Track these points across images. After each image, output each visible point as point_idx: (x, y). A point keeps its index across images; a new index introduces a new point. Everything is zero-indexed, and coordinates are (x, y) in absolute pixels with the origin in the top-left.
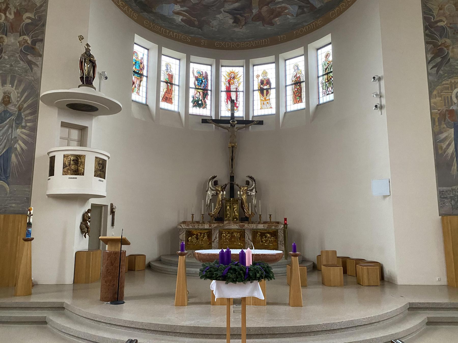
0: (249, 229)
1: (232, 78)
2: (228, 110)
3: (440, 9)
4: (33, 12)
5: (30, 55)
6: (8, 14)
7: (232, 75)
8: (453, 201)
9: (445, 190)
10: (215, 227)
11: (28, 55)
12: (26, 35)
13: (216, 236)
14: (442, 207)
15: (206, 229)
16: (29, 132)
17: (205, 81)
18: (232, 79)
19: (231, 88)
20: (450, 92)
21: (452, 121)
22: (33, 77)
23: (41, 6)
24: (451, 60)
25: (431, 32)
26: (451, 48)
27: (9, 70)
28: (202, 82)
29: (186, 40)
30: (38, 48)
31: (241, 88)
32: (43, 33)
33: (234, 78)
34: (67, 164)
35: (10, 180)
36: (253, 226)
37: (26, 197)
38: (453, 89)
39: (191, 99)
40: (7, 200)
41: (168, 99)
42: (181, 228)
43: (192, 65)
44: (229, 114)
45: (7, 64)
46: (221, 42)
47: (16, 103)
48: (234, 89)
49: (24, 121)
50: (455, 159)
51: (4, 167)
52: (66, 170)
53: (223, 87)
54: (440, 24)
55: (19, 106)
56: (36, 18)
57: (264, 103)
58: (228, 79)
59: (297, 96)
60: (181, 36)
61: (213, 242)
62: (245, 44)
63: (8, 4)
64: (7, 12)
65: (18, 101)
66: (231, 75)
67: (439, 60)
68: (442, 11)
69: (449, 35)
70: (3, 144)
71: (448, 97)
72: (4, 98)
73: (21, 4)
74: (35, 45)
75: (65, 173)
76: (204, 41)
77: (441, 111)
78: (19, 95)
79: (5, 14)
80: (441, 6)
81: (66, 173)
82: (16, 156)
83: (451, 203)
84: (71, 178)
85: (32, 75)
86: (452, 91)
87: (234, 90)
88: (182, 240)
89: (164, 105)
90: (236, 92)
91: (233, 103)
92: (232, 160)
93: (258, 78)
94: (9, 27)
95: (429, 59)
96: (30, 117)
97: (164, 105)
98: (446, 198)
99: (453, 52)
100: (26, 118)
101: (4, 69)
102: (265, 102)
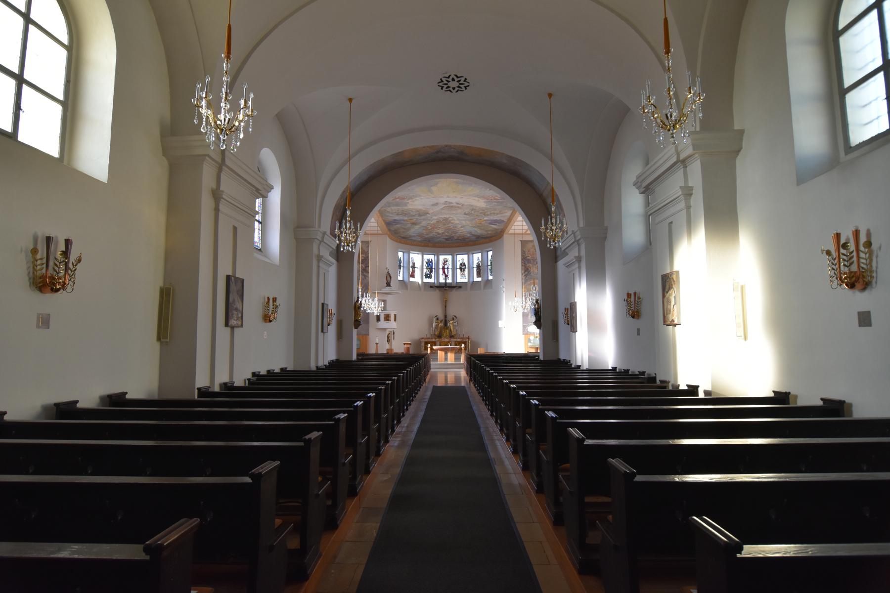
1: (445, 262)
3: (529, 251)
31: (450, 267)
33: (446, 261)
36: (455, 340)
39: (424, 274)
41: (413, 276)
43: (424, 256)
44: (444, 281)
53: (441, 267)
54: (528, 258)
59: (479, 275)
67: (526, 273)
75: (385, 320)
89: (412, 279)
91: (446, 276)
92: (446, 307)
97: (412, 279)
102: (463, 275)
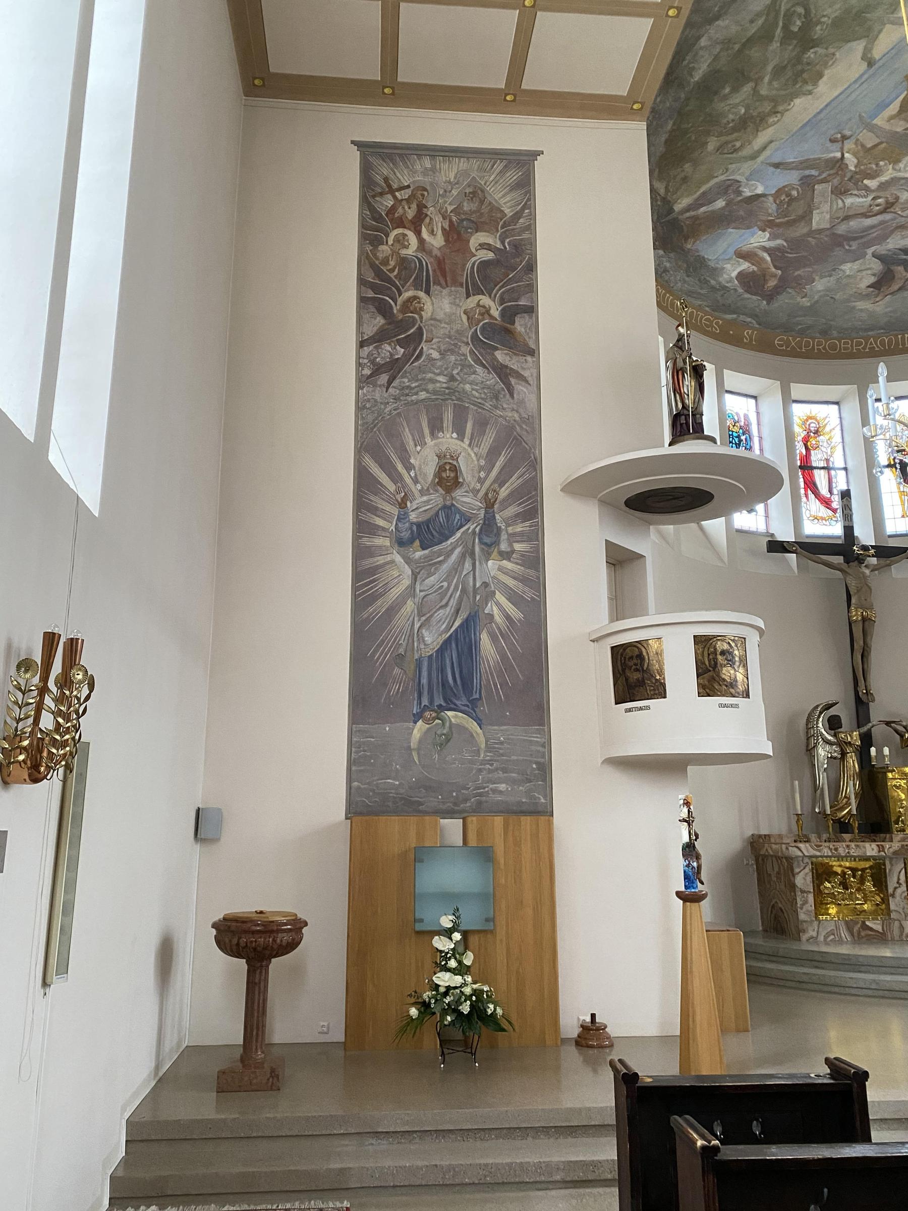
2: (811, 518)
4: (498, 231)
5: (501, 349)
6: (425, 234)
7: (812, 425)
10: (895, 853)
11: (497, 349)
12: (483, 294)
13: (899, 879)
15: (867, 859)
16: (522, 568)
17: (746, 439)
18: (812, 434)
19: (813, 458)
22: (517, 412)
23: (517, 216)
27: (447, 391)
28: (740, 441)
29: (712, 329)
30: (523, 330)
32: (531, 288)
33: (817, 432)
34: (707, 663)
35: (484, 708)
37: (536, 763)
40: (480, 770)
42: (800, 854)
45: (439, 375)
46: (790, 338)
47: (478, 486)
48: (822, 462)
49: (504, 536)
51: (461, 672)
52: (706, 683)
55: (486, 494)
56: (507, 247)
58: (803, 435)
60: (702, 317)
61: (893, 895)
62: (852, 346)
63: (421, 207)
64: (424, 229)
65: (481, 481)
66: (809, 425)
70: (453, 602)
72: (441, 469)
73: (459, 207)
74: (513, 323)
76: (750, 332)
78: (482, 462)
79: (418, 233)
81: (708, 691)
82: (493, 638)
84: (725, 706)
85: (515, 406)
87: (822, 465)
88: (802, 891)
90: (827, 471)
94: (434, 271)
96: (521, 525)
100: (510, 529)
101: (430, 387)
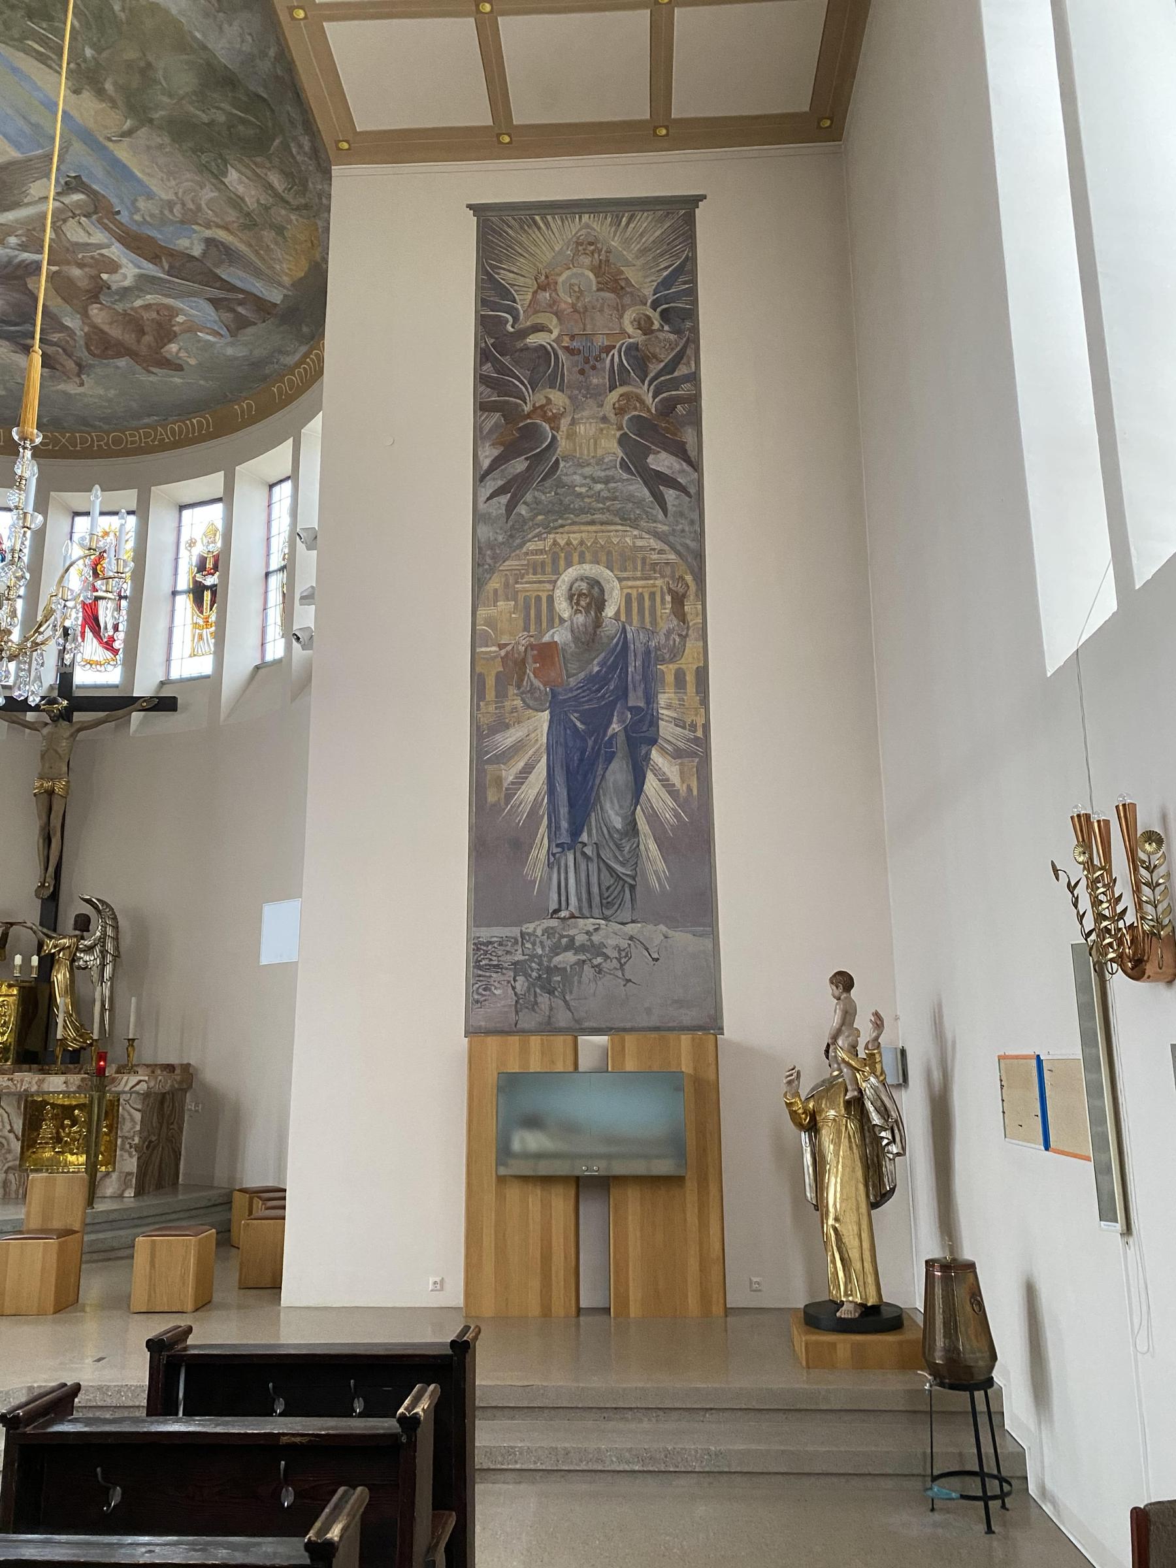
0: (13, 1094)
2: (83, 663)
3: (542, 288)
8: (520, 979)
9: (495, 939)
14: (477, 1002)
20: (549, 582)
21: (545, 685)
24: (562, 464)
25: (502, 369)
26: (564, 423)
38: (562, 568)
50: (545, 821)
54: (534, 340)
57: (201, 637)
62: (140, 437)
67: (519, 465)
68: (548, 294)
69: (563, 375)
71: (538, 598)
77: (509, 648)
80: (543, 277)
83: (514, 988)
86: (554, 577)
93: (190, 551)
95: (486, 464)
98: (498, 967)
99: (571, 436)
